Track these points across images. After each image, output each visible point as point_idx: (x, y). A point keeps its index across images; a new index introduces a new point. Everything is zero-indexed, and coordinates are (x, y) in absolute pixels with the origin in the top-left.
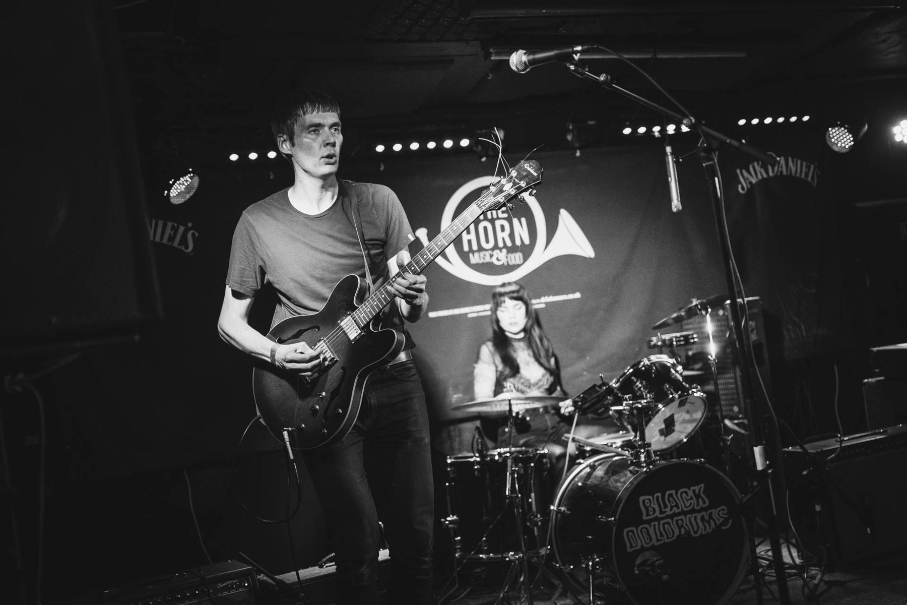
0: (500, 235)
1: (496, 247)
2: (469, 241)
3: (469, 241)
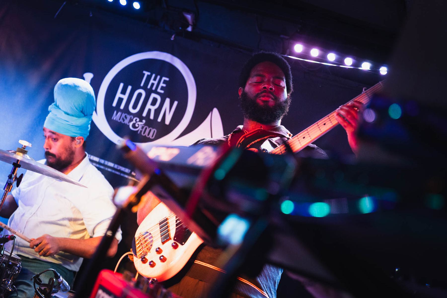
0: (149, 106)
1: (139, 115)
2: (121, 100)
3: (121, 100)
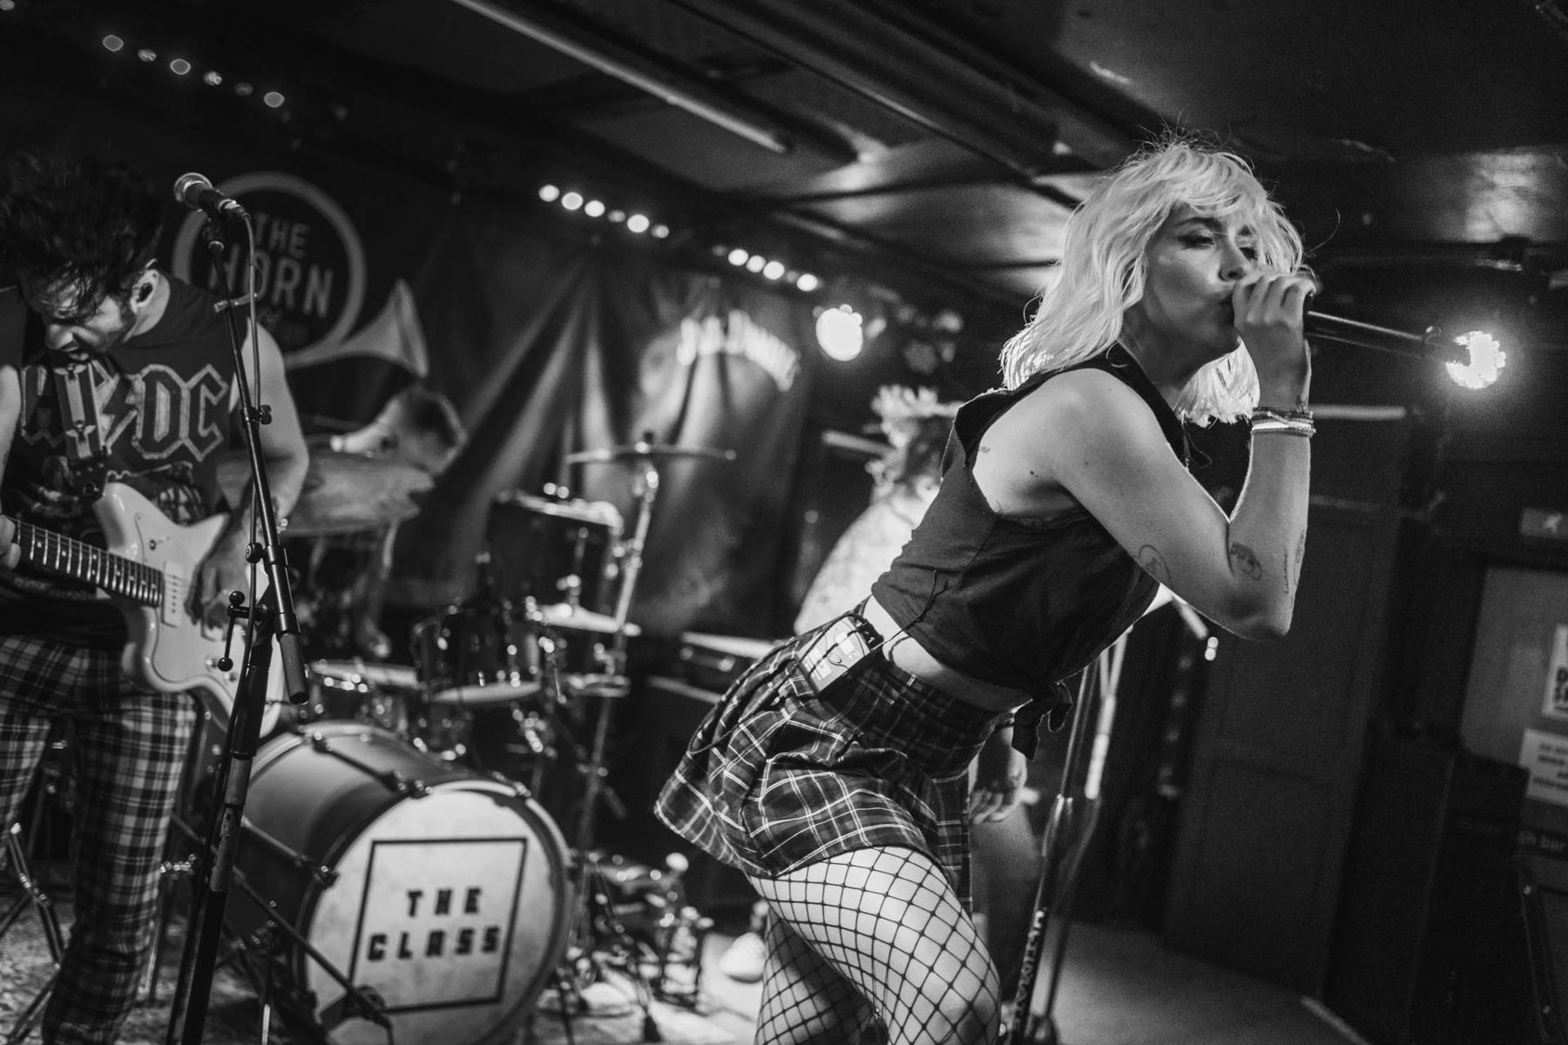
0: (280, 284)
